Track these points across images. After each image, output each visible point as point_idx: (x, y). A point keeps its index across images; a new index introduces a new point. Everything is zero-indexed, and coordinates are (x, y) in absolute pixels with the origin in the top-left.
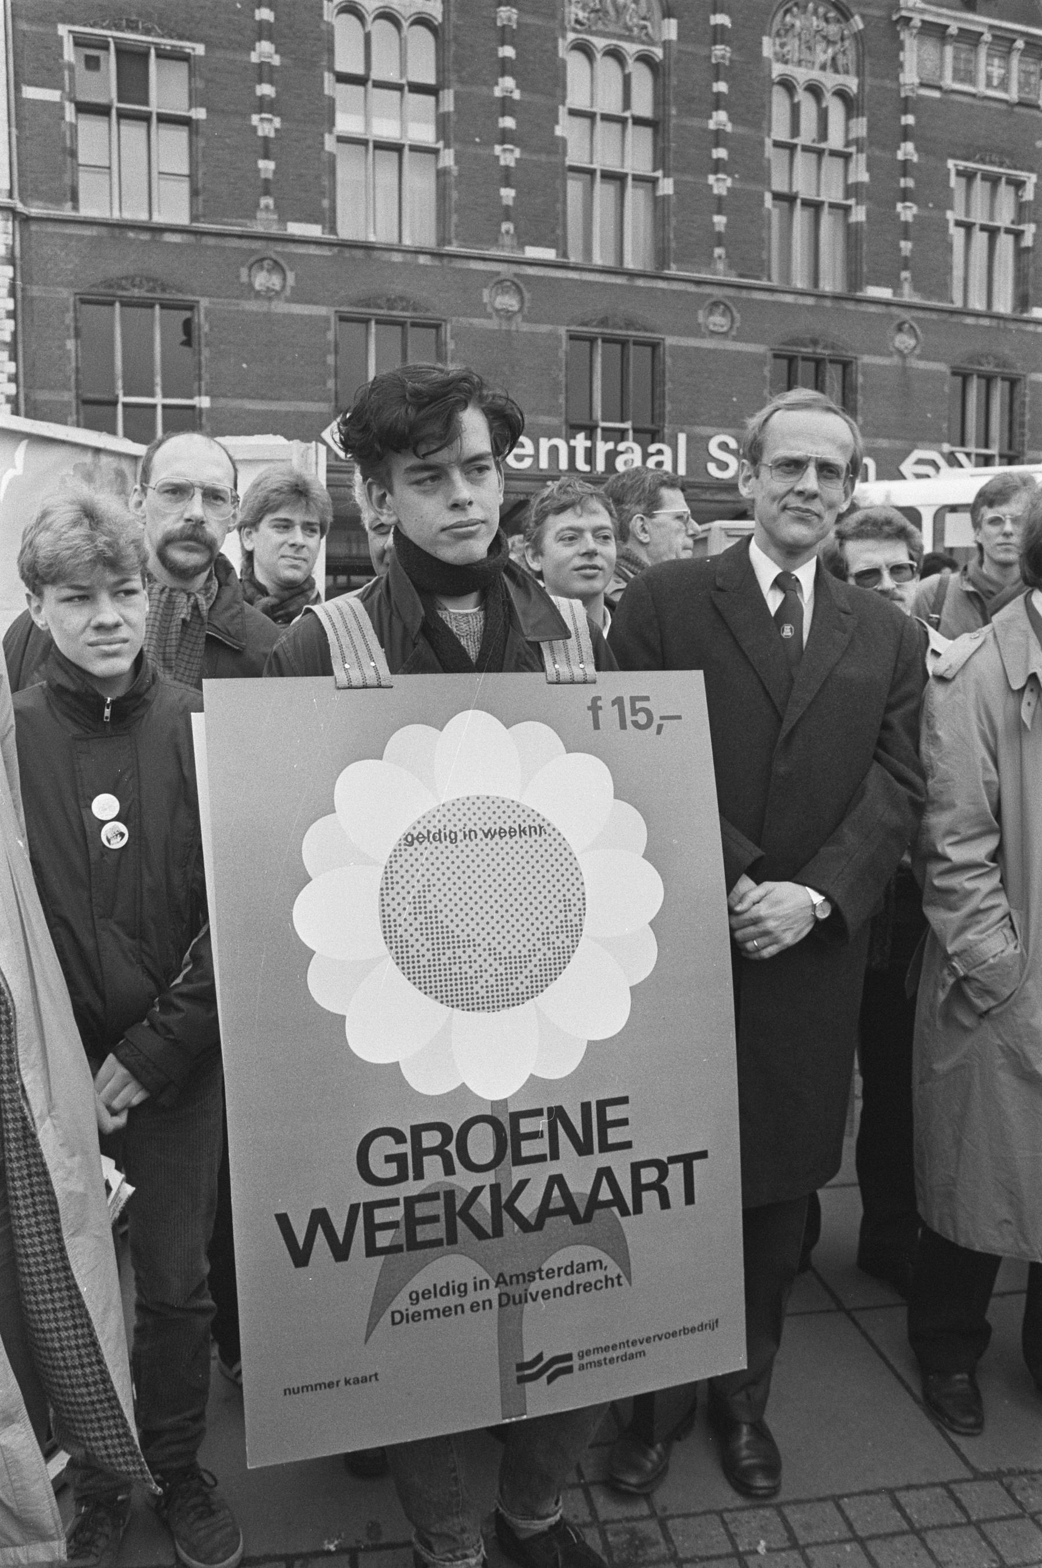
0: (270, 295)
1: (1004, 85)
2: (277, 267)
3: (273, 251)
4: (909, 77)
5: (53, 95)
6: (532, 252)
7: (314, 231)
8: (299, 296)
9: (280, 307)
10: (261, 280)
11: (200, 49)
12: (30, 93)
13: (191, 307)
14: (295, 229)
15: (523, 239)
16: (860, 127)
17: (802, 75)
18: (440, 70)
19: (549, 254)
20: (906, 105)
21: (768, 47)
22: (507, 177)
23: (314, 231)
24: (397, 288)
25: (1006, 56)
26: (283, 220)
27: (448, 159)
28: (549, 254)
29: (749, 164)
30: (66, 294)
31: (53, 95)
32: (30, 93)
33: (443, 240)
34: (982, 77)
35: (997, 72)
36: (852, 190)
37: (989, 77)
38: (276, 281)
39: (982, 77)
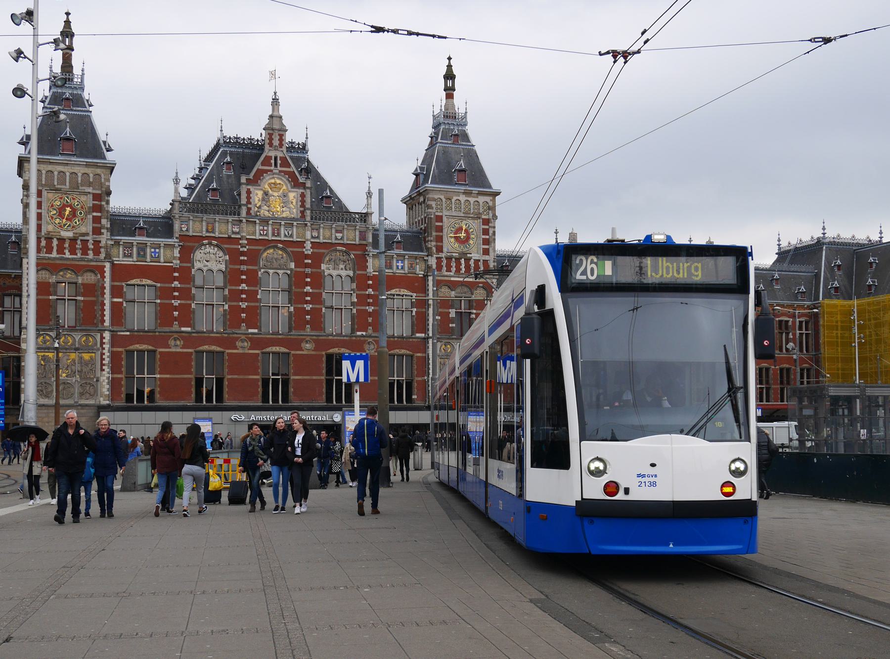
1: (403, 268)
4: (370, 269)
5: (120, 300)
6: (250, 331)
12: (115, 300)
14: (183, 329)
15: (248, 327)
16: (354, 286)
17: (334, 273)
18: (225, 283)
19: (256, 331)
20: (369, 278)
21: (323, 266)
22: (243, 311)
25: (403, 261)
26: (180, 327)
28: (256, 331)
29: (317, 299)
31: (120, 300)
32: (115, 300)
34: (395, 267)
35: (400, 264)
36: (353, 304)
37: (397, 267)
39: (395, 267)
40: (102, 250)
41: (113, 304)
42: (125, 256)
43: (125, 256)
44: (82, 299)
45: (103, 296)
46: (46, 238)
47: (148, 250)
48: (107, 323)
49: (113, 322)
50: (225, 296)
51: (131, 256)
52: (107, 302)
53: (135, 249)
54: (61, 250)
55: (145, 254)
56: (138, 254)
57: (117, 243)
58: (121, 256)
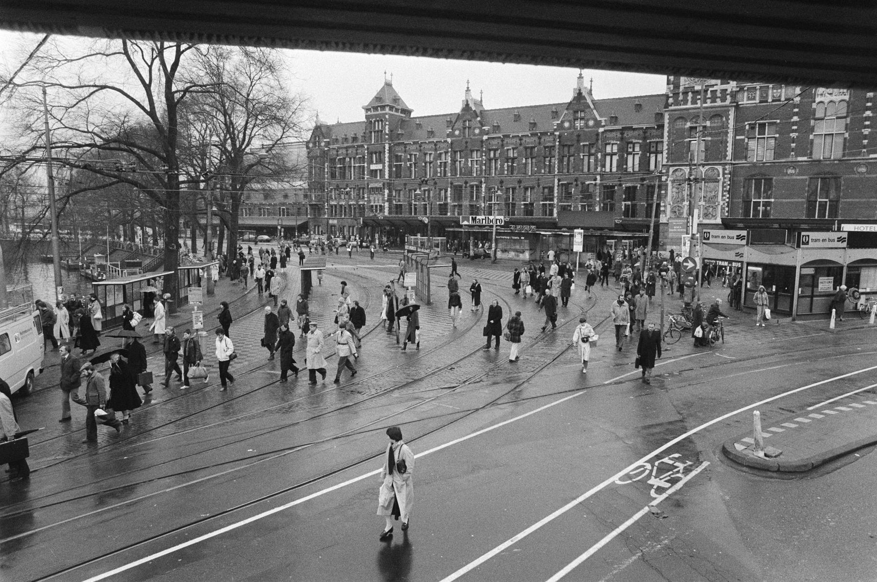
0: (792, 174)
2: (794, 168)
3: (794, 165)
5: (742, 137)
7: (805, 159)
8: (799, 175)
9: (795, 177)
10: (790, 171)
11: (778, 121)
12: (738, 138)
13: (771, 179)
14: (800, 159)
22: (865, 137)
23: (805, 159)
24: (827, 170)
26: (796, 156)
27: (847, 135)
30: (742, 179)
31: (742, 137)
32: (738, 138)
33: (844, 155)
38: (793, 171)
40: (728, 97)
41: (736, 143)
42: (749, 99)
43: (749, 99)
44: (710, 139)
45: (727, 136)
46: (683, 93)
47: (770, 91)
48: (729, 157)
49: (735, 156)
50: (847, 125)
51: (754, 99)
52: (730, 140)
53: (758, 92)
54: (694, 102)
55: (767, 95)
56: (761, 96)
57: (742, 89)
58: (745, 99)
